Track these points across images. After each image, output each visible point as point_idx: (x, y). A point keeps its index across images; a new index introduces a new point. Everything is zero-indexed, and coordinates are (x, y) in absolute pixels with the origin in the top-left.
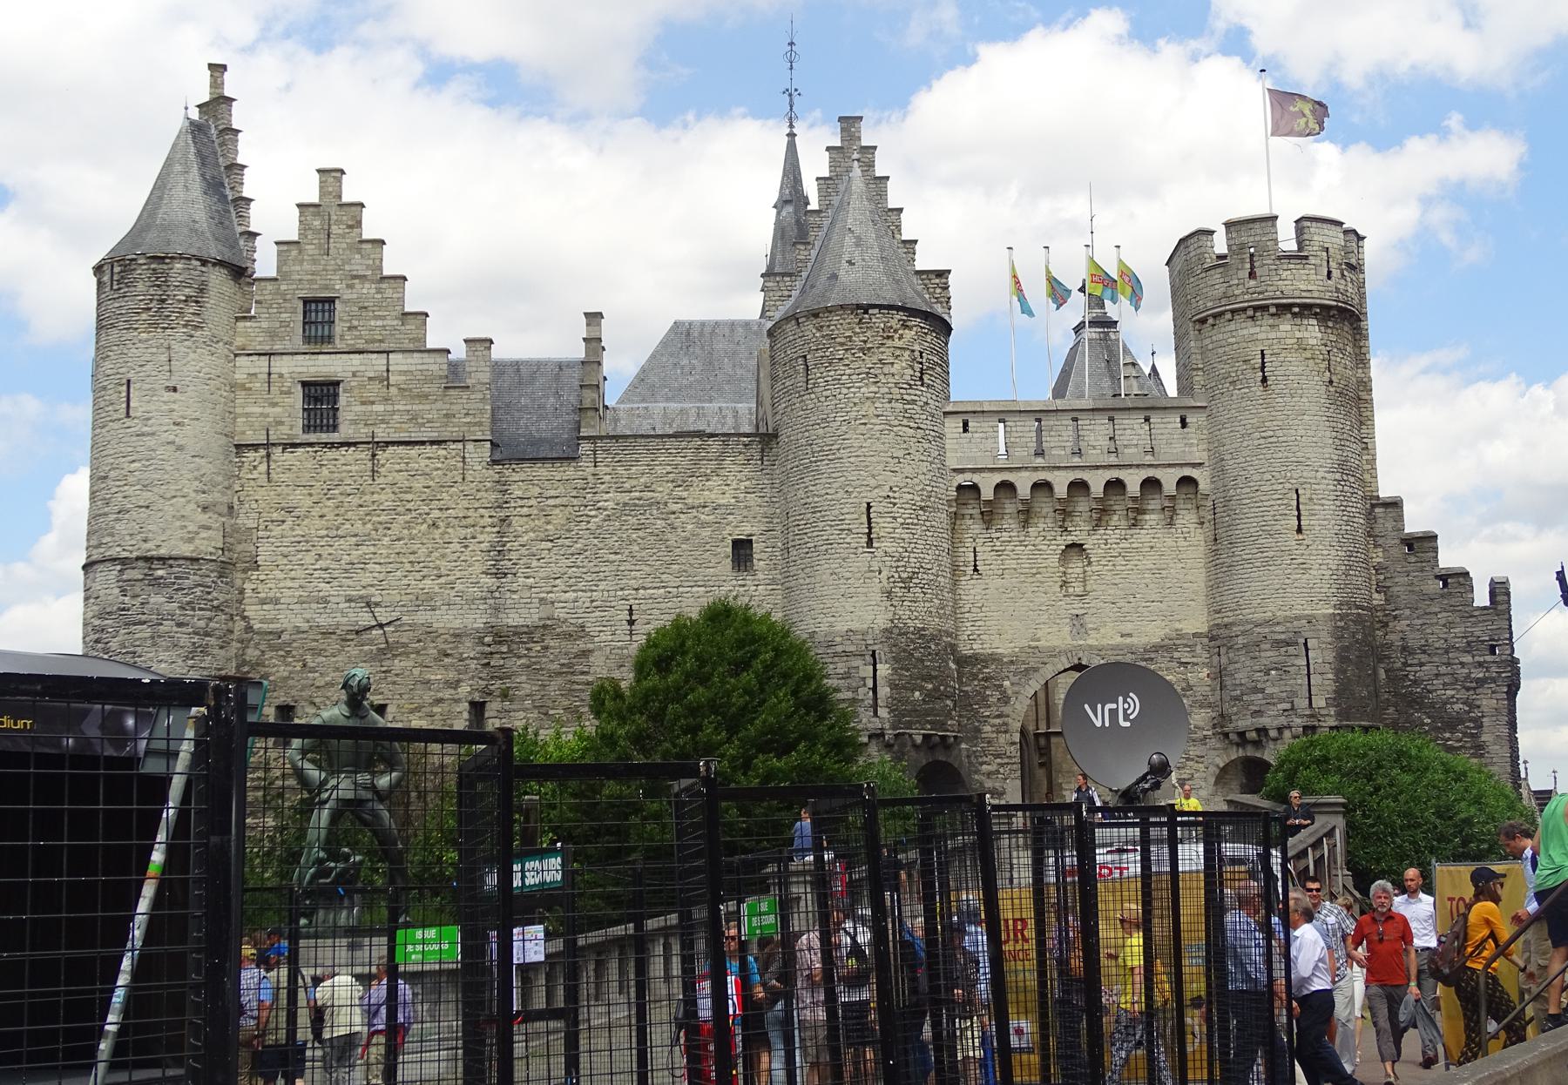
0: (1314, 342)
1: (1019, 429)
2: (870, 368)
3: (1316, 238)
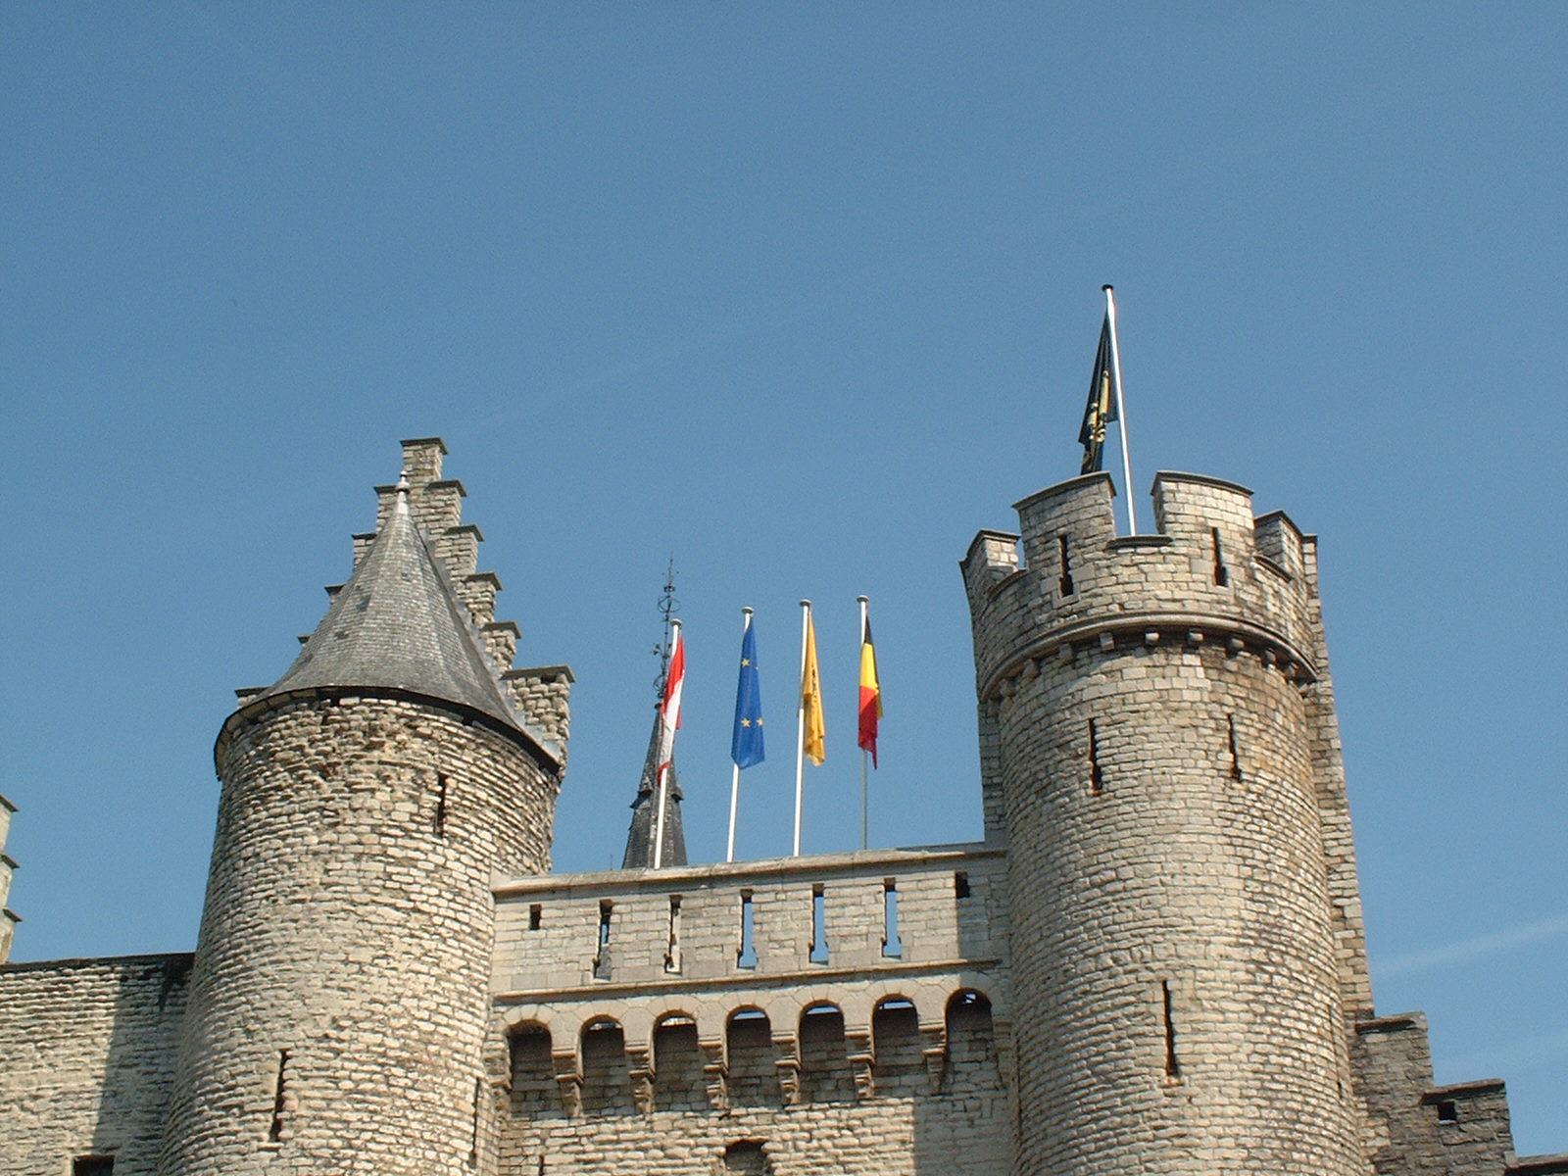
0: (1187, 695)
1: (636, 917)
2: (327, 800)
3: (1188, 509)
